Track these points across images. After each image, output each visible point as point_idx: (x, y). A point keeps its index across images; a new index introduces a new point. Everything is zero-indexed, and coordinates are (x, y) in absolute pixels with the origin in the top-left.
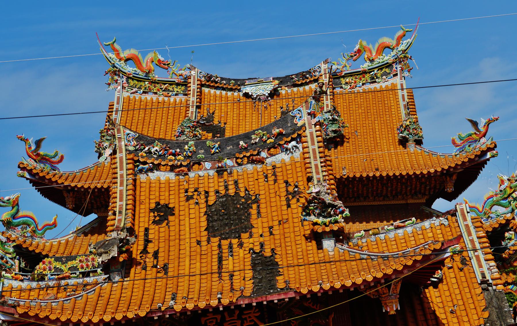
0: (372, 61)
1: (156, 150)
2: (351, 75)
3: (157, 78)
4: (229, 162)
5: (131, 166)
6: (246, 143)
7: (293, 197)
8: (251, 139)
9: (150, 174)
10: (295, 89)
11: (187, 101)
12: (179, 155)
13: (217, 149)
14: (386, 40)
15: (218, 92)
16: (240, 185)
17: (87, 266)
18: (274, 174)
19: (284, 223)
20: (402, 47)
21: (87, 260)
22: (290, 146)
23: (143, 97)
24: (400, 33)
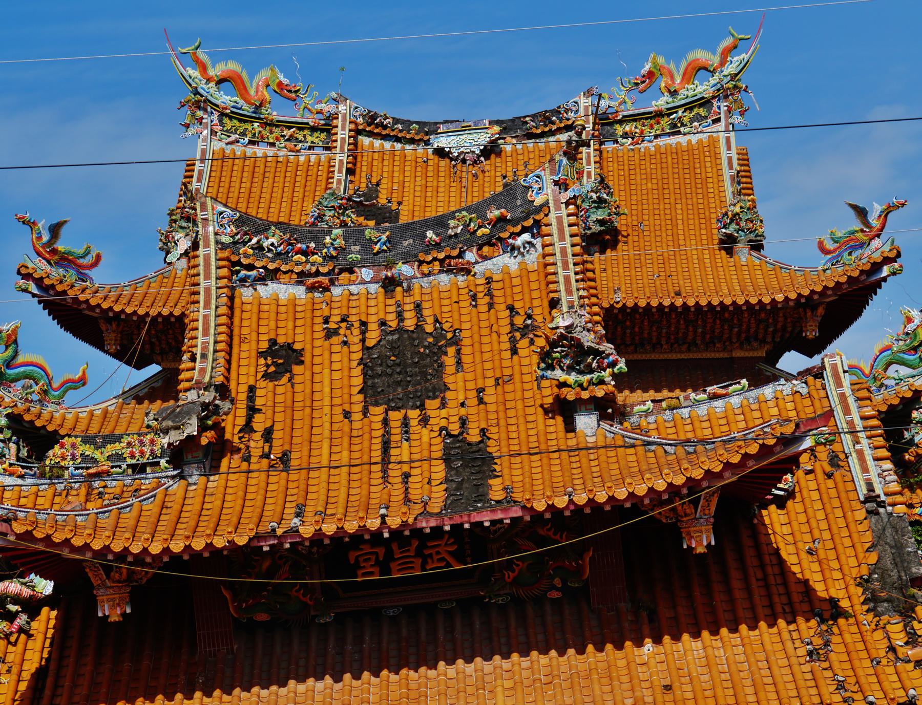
0: (674, 93)
1: (272, 244)
2: (634, 118)
3: (275, 116)
4: (405, 269)
5: (224, 272)
6: (437, 235)
7: (523, 336)
8: (447, 227)
9: (258, 287)
10: (530, 144)
11: (330, 160)
12: (313, 254)
13: (384, 244)
15: (388, 145)
16: (426, 312)
17: (142, 453)
18: (489, 293)
19: (505, 383)
20: (730, 69)
21: (142, 443)
22: (519, 241)
23: (250, 151)
24: (728, 42)
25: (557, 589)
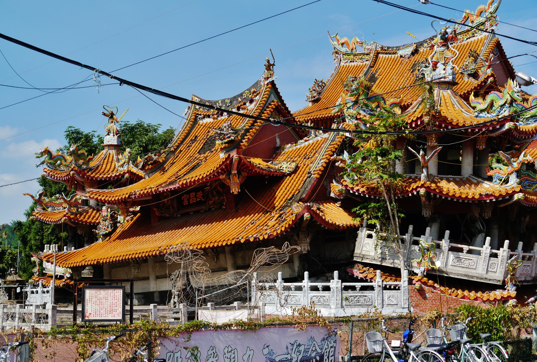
14: (482, 7)
15: (387, 56)
20: (492, 10)
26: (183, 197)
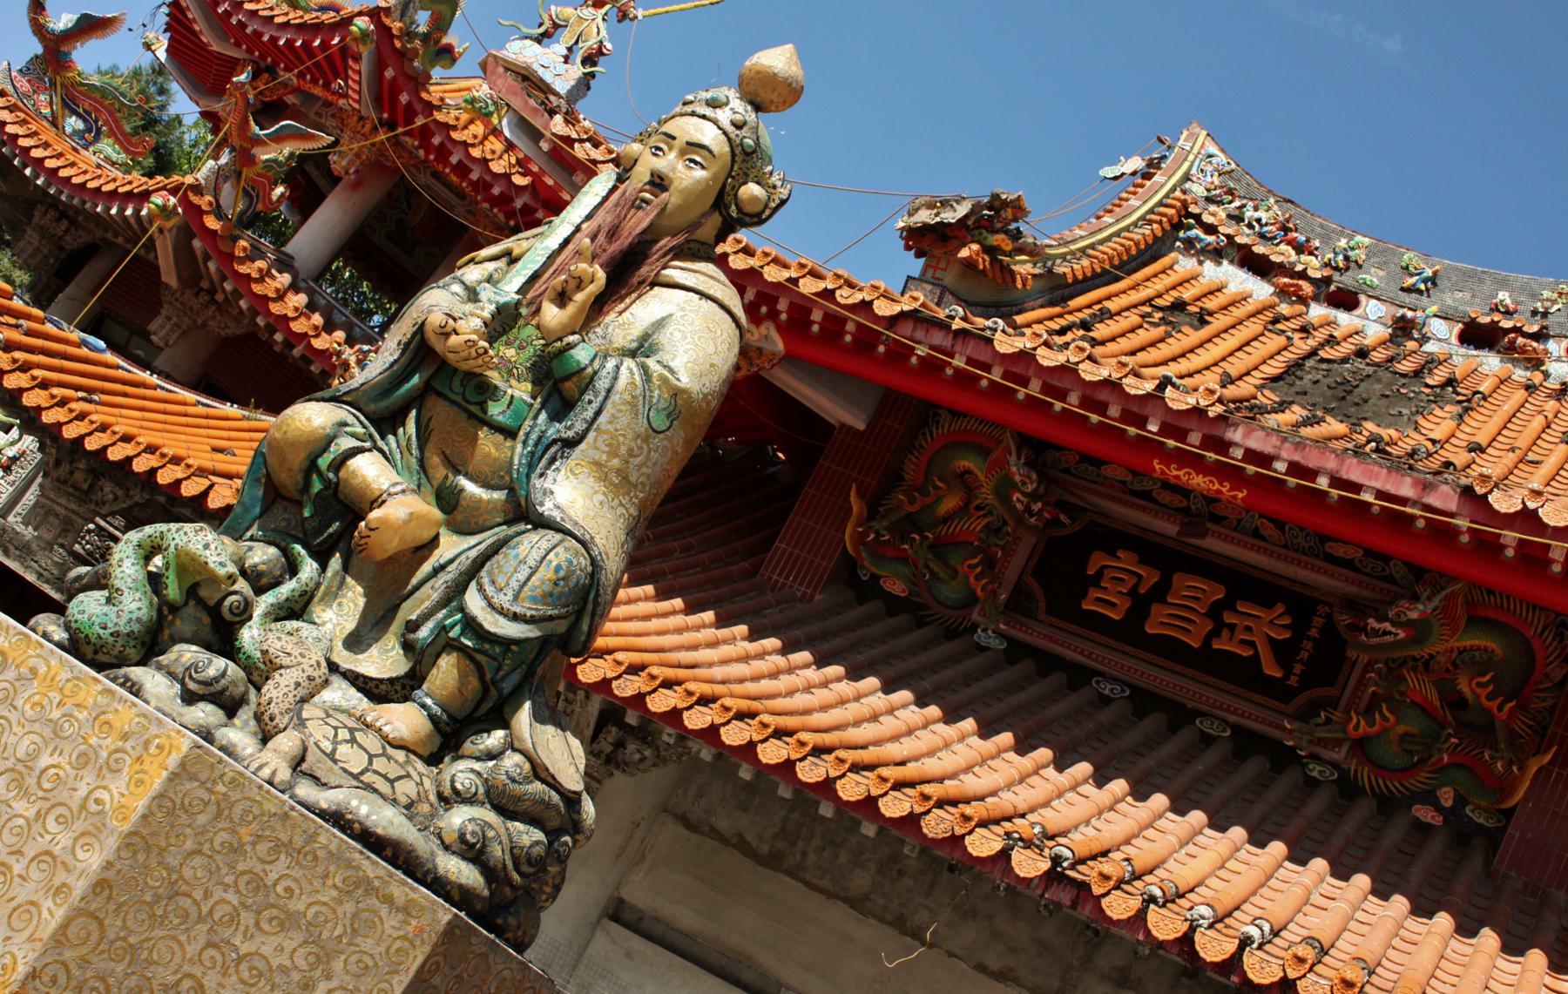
13: (1425, 281)
25: (1439, 808)
26: (1098, 560)
